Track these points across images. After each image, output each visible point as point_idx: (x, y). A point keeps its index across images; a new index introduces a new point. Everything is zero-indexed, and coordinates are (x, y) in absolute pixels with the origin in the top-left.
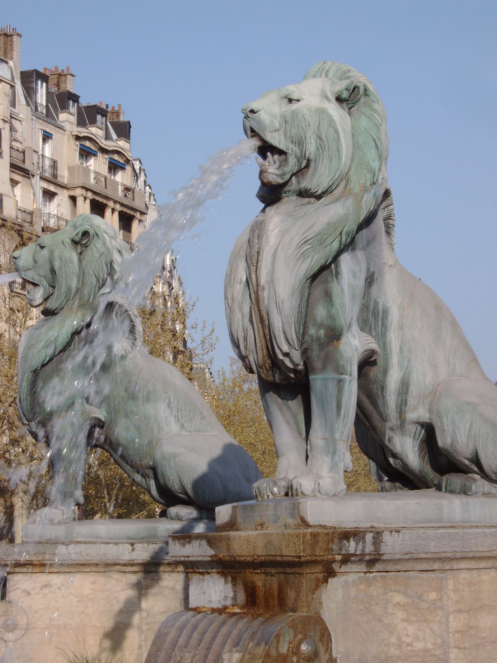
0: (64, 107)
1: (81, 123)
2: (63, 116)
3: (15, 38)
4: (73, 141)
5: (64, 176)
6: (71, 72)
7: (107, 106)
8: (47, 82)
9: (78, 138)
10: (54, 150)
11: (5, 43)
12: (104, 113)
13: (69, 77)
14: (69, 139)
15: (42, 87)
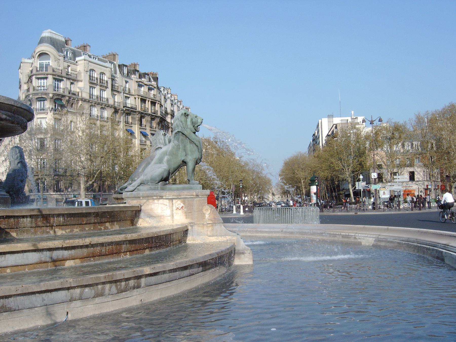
0: (135, 74)
1: (140, 77)
2: (132, 76)
3: (116, 56)
4: (135, 83)
5: (133, 92)
6: (138, 64)
7: (154, 73)
8: (127, 67)
9: (137, 82)
10: (129, 85)
11: (114, 57)
12: (148, 75)
13: (137, 65)
14: (134, 82)
15: (125, 68)
